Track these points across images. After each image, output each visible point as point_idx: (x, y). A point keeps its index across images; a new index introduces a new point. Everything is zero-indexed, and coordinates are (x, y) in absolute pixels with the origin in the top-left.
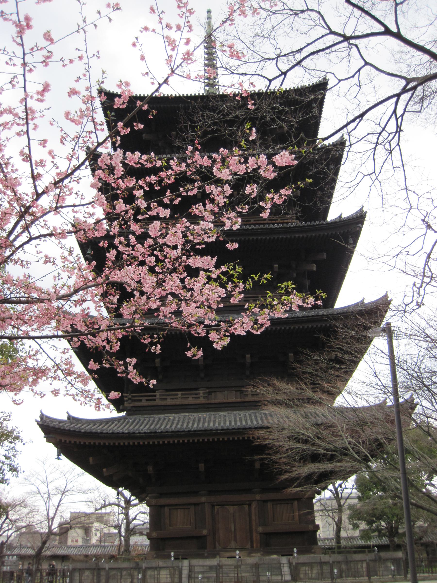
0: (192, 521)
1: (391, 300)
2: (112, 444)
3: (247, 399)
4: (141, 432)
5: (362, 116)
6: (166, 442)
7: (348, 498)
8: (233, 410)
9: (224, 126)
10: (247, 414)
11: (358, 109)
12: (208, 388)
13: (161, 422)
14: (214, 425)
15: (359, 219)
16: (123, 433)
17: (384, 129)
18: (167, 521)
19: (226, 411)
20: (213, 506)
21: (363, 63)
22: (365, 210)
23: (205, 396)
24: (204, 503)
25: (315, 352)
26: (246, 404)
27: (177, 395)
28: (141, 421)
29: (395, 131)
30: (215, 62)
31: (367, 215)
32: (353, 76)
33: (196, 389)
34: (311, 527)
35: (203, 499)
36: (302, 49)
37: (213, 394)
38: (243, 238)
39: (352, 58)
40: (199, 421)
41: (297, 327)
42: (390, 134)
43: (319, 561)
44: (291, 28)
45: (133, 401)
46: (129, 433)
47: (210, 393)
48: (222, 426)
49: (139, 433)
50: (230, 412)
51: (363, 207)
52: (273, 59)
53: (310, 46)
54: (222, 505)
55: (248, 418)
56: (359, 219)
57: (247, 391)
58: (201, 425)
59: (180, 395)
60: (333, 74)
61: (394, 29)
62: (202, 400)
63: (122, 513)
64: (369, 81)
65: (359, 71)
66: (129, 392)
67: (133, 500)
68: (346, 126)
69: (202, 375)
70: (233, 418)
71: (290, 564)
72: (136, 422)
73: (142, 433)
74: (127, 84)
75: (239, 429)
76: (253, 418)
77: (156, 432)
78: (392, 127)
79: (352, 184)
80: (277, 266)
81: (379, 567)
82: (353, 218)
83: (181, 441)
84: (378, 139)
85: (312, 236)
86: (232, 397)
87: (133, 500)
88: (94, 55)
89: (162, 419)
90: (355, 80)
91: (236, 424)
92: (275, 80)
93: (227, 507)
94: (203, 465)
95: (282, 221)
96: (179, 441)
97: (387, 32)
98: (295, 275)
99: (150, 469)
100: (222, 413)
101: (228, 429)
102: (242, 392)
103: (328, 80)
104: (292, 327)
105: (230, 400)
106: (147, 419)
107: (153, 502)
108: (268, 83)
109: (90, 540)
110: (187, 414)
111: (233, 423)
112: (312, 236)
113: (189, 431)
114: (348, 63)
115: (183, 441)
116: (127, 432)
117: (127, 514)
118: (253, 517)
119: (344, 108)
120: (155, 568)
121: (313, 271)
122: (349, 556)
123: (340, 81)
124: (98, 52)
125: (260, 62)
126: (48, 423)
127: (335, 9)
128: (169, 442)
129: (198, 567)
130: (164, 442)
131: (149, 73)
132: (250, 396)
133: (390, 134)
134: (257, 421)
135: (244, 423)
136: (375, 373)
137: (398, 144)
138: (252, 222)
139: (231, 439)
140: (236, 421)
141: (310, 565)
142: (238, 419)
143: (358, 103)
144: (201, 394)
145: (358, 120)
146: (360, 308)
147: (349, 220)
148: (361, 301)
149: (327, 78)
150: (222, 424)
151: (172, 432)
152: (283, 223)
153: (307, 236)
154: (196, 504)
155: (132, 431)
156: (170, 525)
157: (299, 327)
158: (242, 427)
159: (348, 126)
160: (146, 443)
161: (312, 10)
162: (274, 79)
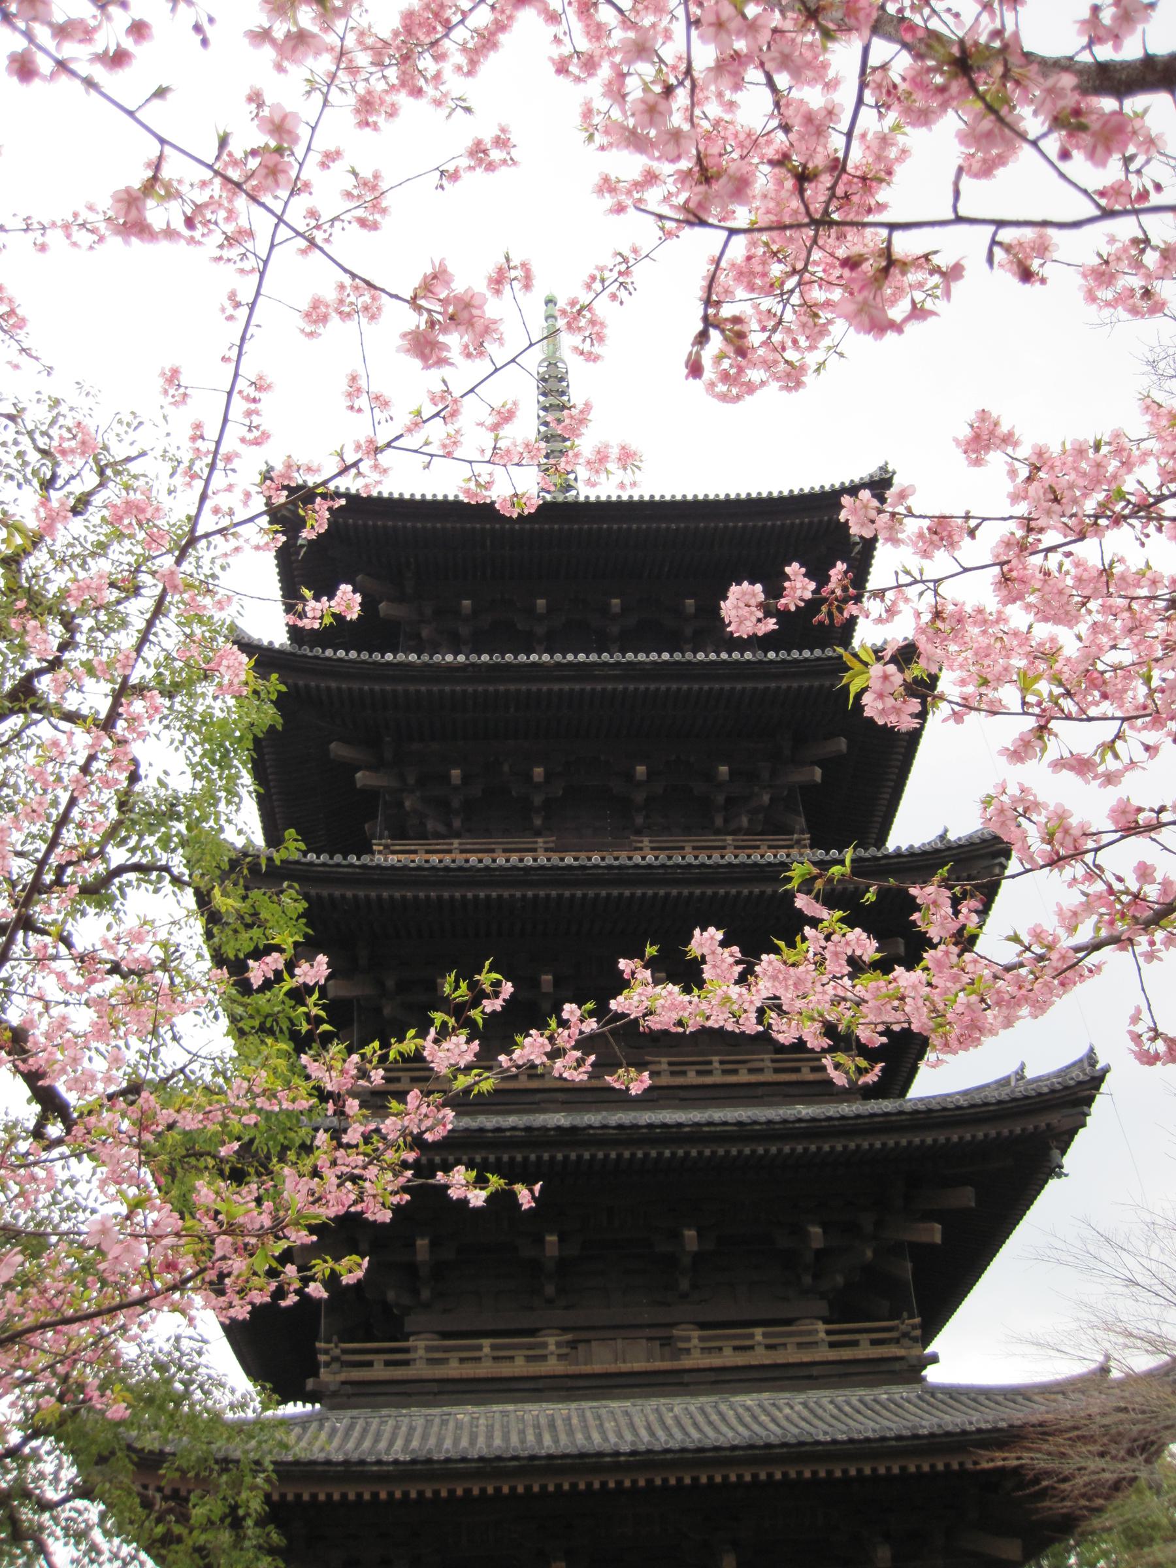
1: (1106, 1070)
2: (290, 1497)
3: (687, 1363)
4: (385, 1458)
12: (565, 1330)
13: (435, 1429)
16: (328, 1462)
19: (626, 1397)
23: (564, 1351)
26: (686, 1378)
27: (480, 1348)
28: (374, 1427)
33: (532, 1332)
37: (582, 1347)
40: (552, 1426)
41: (839, 1148)
46: (346, 1463)
47: (573, 1344)
49: (379, 1462)
50: (639, 1402)
59: (487, 1350)
62: (554, 1366)
66: (335, 1338)
69: (550, 1290)
73: (388, 1463)
75: (683, 1450)
76: (714, 1417)
77: (429, 1461)
83: (506, 1490)
86: (639, 1359)
89: (437, 1420)
96: (498, 1490)
100: (614, 1404)
101: (649, 1451)
102: (667, 1342)
103: (894, 473)
104: (826, 1148)
106: (391, 1422)
110: (510, 1407)
113: (533, 1458)
115: (513, 1489)
116: (341, 1458)
128: (468, 1491)
130: (452, 1492)
132: (696, 1353)
142: (670, 1422)
147: (972, 844)
148: (1017, 1073)
149: (890, 468)
155: (355, 1457)
157: (845, 1147)
158: (691, 1446)
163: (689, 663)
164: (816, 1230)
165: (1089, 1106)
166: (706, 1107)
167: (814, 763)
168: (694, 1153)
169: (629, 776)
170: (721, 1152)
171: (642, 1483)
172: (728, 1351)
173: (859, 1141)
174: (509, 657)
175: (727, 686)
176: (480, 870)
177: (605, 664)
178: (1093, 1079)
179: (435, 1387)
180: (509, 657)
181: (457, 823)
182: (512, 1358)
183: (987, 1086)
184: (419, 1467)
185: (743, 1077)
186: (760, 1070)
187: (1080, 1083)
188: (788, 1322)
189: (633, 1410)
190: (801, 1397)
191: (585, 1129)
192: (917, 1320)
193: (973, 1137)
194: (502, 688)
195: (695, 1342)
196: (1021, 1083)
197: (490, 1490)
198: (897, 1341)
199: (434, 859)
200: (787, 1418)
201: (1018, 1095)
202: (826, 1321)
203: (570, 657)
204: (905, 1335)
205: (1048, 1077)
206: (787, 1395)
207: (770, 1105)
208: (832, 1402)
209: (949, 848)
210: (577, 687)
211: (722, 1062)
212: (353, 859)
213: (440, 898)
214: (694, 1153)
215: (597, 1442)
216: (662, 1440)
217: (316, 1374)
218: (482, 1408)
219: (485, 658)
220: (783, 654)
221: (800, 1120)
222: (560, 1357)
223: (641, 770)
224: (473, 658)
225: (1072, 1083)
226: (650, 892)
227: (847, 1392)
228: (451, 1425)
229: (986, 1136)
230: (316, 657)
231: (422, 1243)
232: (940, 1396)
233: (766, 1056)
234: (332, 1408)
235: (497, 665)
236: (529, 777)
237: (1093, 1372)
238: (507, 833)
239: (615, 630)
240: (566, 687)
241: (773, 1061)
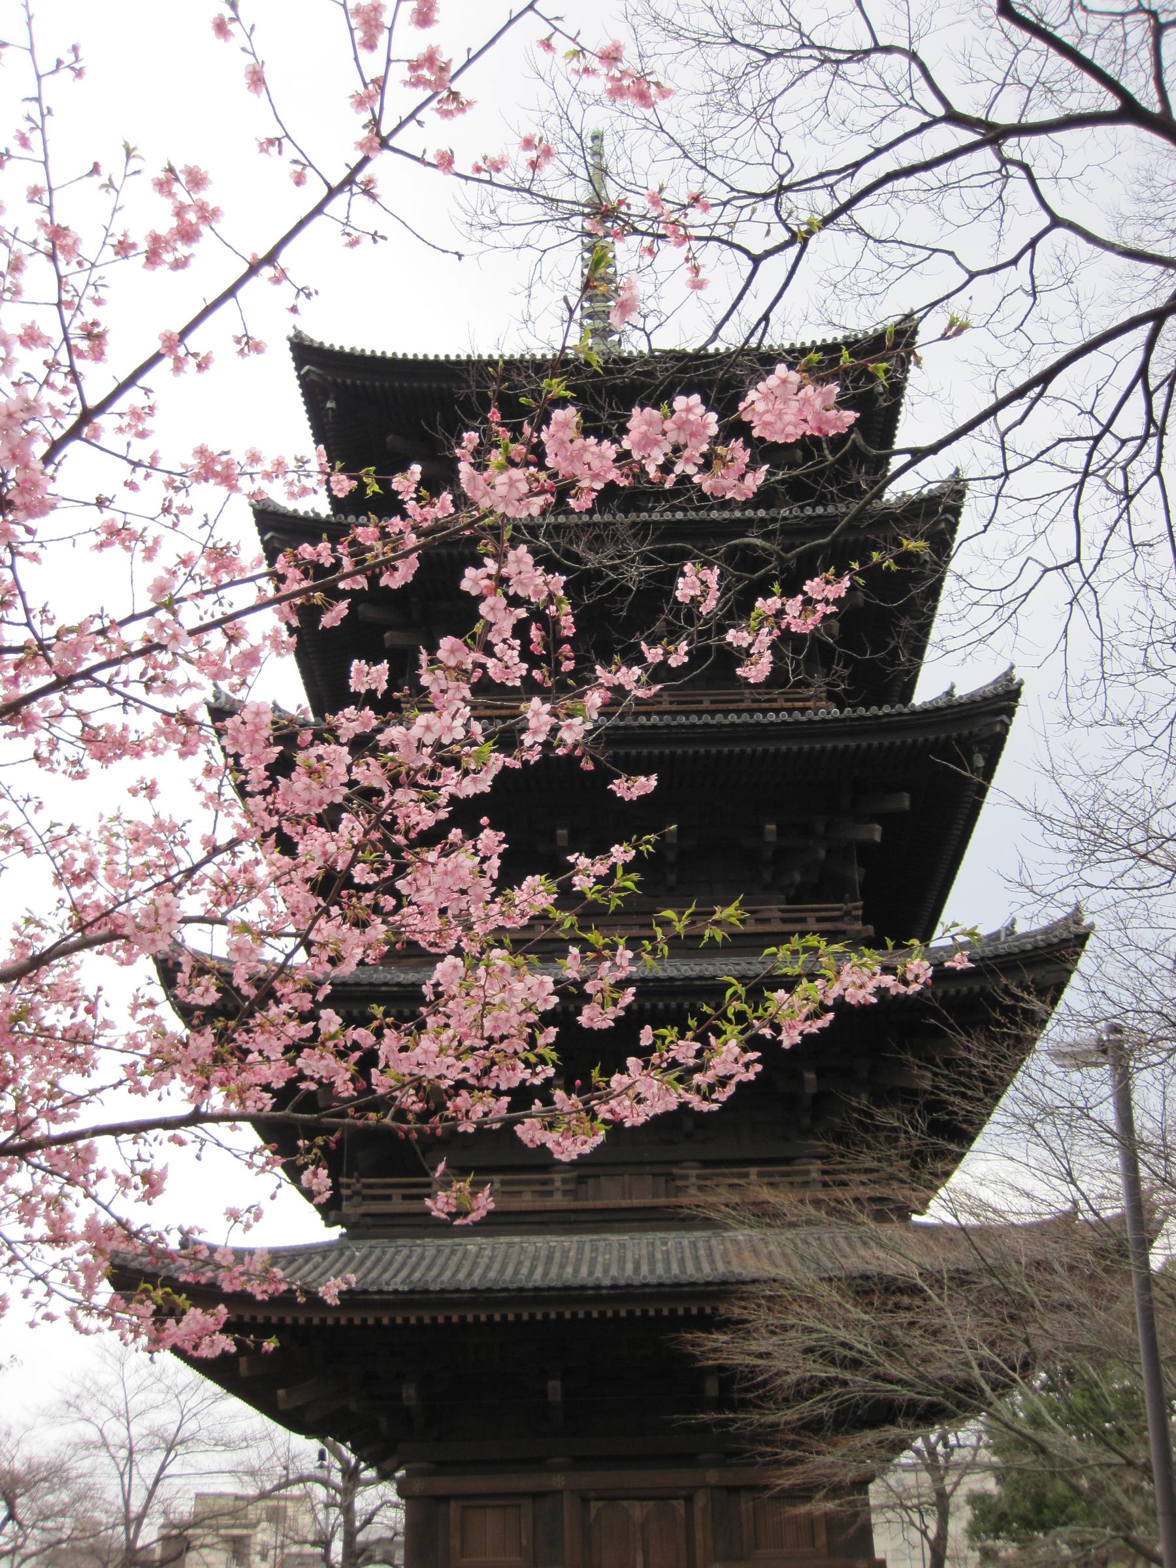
0: (524, 1542)
4: (386, 1288)
5: (1046, 378)
6: (455, 1319)
8: (645, 1230)
9: (610, 405)
10: (685, 1242)
11: (1024, 366)
13: (441, 1260)
14: (591, 1273)
15: (1002, 700)
17: (1106, 429)
18: (456, 1542)
20: (585, 1501)
21: (1046, 221)
22: (1017, 675)
24: (561, 1492)
25: (886, 1106)
28: (388, 1257)
29: (1140, 432)
31: (1023, 689)
32: (1014, 262)
35: (558, 1481)
36: (857, 165)
37: (591, 1182)
38: (679, 751)
39: (1010, 210)
40: (550, 1258)
42: (1124, 442)
44: (821, 114)
45: (365, 1198)
48: (614, 1278)
49: (380, 1292)
50: (637, 1235)
51: (1012, 667)
52: (765, 196)
53: (885, 155)
54: (611, 1497)
55: (688, 1253)
56: (1002, 700)
58: (554, 1270)
60: (951, 253)
61: (1149, 101)
62: (558, 1201)
64: (1062, 281)
65: (1032, 244)
66: (356, 1174)
68: (992, 412)
70: (644, 1252)
72: (373, 1258)
73: (388, 1293)
74: (196, 180)
75: (660, 1285)
76: (702, 1252)
77: (427, 1291)
78: (1132, 422)
79: (1007, 595)
80: (773, 827)
82: (985, 699)
83: (497, 1318)
84: (1090, 455)
85: (870, 746)
88: (59, 63)
89: (447, 1251)
90: (1018, 276)
91: (652, 1271)
92: (770, 259)
93: (625, 1503)
95: (789, 705)
96: (490, 1317)
97: (1130, 112)
98: (822, 853)
99: (409, 1393)
100: (614, 1238)
101: (629, 1286)
105: (636, 1202)
106: (405, 1252)
107: (418, 1486)
108: (749, 265)
110: (517, 1239)
111: (645, 1269)
112: (870, 746)
113: (521, 1290)
114: (998, 224)
118: (699, 1536)
119: (983, 362)
121: (875, 843)
123: (973, 275)
124: (75, 49)
125: (725, 204)
126: (124, 1259)
127: (961, 58)
128: (463, 1319)
130: (448, 1319)
131: (285, 141)
132: (693, 1191)
133: (1124, 442)
134: (712, 1262)
135: (675, 1269)
136: (1069, 1174)
137: (1157, 472)
138: (706, 705)
139: (638, 1313)
140: (652, 1261)
142: (658, 1256)
143: (1026, 345)
144: (558, 1184)
145: (1033, 393)
146: (1003, 948)
147: (974, 702)
150: (614, 1271)
151: (473, 1290)
152: (790, 711)
153: (859, 746)
154: (537, 1496)
158: (668, 1281)
159: (1000, 414)
160: (399, 1320)
161: (888, 50)
162: (768, 253)
163: (703, 522)
164: (810, 1076)
171: (623, 1313)
178: (1077, 936)
182: (520, 1192)
186: (767, 921)
187: (1063, 941)
188: (788, 1161)
189: (629, 1243)
193: (958, 991)
195: (693, 1180)
196: (1010, 938)
197: (483, 1318)
204: (892, 1177)
209: (951, 707)
215: (584, 1275)
216: (645, 1274)
222: (565, 1193)
225: (1055, 940)
226: (656, 751)
228: (459, 1255)
229: (971, 990)
241: (782, 911)
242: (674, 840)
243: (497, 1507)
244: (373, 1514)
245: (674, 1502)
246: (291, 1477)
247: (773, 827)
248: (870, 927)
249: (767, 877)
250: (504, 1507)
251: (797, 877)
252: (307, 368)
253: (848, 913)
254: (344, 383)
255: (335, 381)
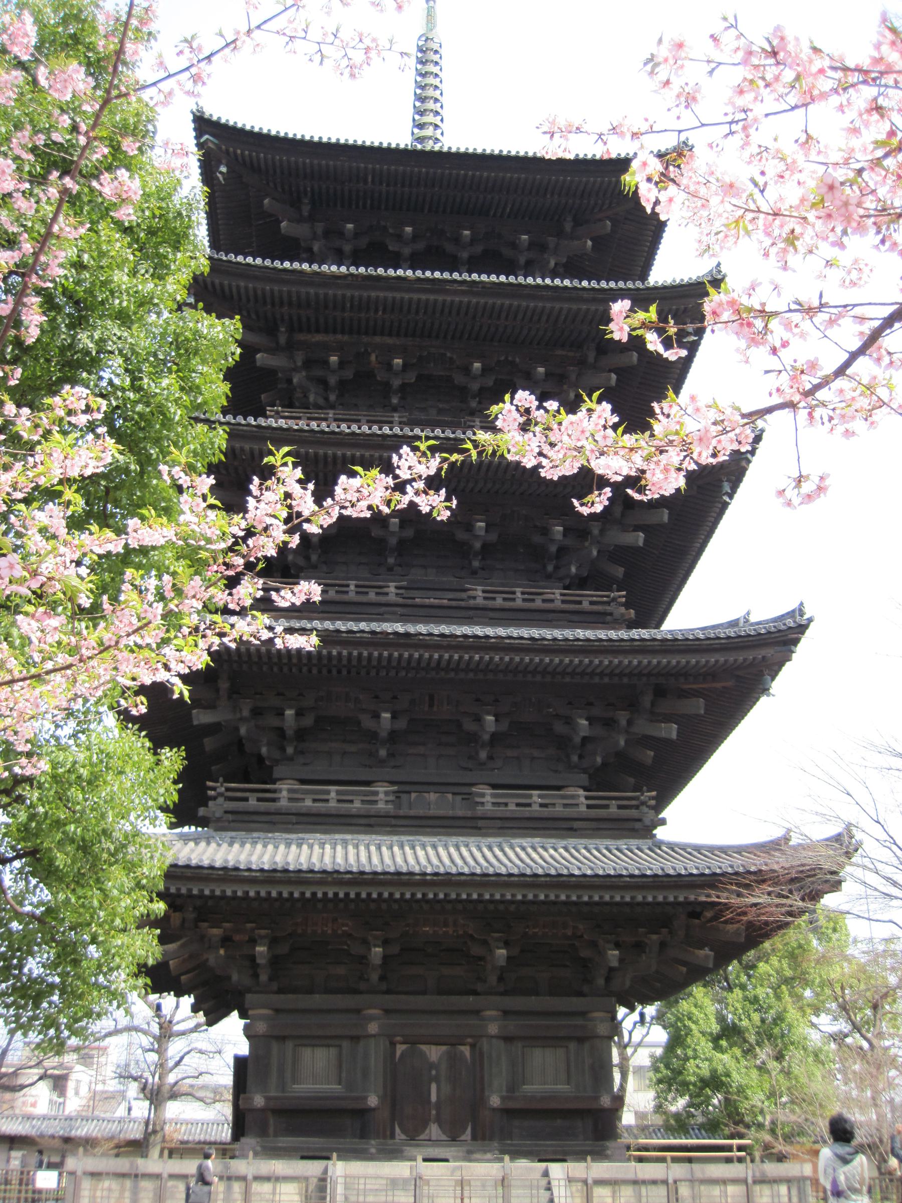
1: (810, 620)
7: (639, 1045)
12: (392, 783)
23: (391, 798)
26: (480, 823)
27: (328, 792)
30: (438, 92)
31: (764, 435)
33: (368, 783)
34: (606, 1101)
43: (631, 1176)
46: (224, 869)
50: (444, 838)
57: (483, 795)
63: (152, 1050)
66: (221, 779)
67: (178, 1023)
69: (383, 753)
71: (570, 1180)
77: (286, 871)
81: (761, 1196)
87: (178, 1023)
93: (423, 1047)
94: (379, 950)
98: (595, 553)
109: (64, 1103)
110: (348, 837)
117: (160, 1051)
120: (268, 1179)
122: (696, 1166)
129: (373, 1181)
141: (613, 1183)
144: (382, 796)
149: (690, 143)
155: (231, 864)
156: (295, 1081)
157: (611, 662)
163: (520, 285)
165: (795, 645)
166: (509, 626)
167: (610, 371)
168: (497, 658)
169: (467, 370)
170: (517, 659)
172: (512, 807)
173: (621, 658)
174: (381, 271)
175: (548, 305)
176: (348, 434)
177: (455, 281)
178: (801, 626)
179: (294, 819)
180: (381, 271)
181: (332, 397)
183: (721, 625)
184: (279, 875)
185: (538, 604)
187: (790, 628)
188: (559, 788)
190: (564, 843)
191: (416, 635)
192: (654, 793)
194: (373, 294)
195: (488, 798)
198: (637, 807)
199: (314, 425)
200: (552, 857)
201: (743, 633)
202: (586, 789)
203: (428, 274)
205: (767, 622)
206: (553, 841)
207: (557, 627)
208: (585, 848)
210: (432, 297)
211: (523, 593)
212: (251, 420)
213: (316, 454)
214: (497, 658)
217: (206, 805)
218: (328, 836)
219: (362, 270)
220: (594, 284)
221: (578, 640)
223: (477, 365)
224: (353, 269)
227: (598, 841)
230: (230, 262)
231: (289, 712)
232: (664, 848)
233: (557, 591)
234: (216, 830)
235: (370, 277)
236: (389, 366)
237: (779, 839)
238: (371, 407)
239: (465, 255)
240: (424, 297)
241: (562, 595)
242: (482, 533)
243: (322, 1046)
244: (182, 1058)
245: (462, 1048)
246: (119, 1027)
247: (561, 529)
248: (632, 611)
249: (550, 568)
250: (328, 1046)
251: (573, 570)
252: (206, 137)
253: (614, 599)
254: (235, 153)
255: (227, 152)
